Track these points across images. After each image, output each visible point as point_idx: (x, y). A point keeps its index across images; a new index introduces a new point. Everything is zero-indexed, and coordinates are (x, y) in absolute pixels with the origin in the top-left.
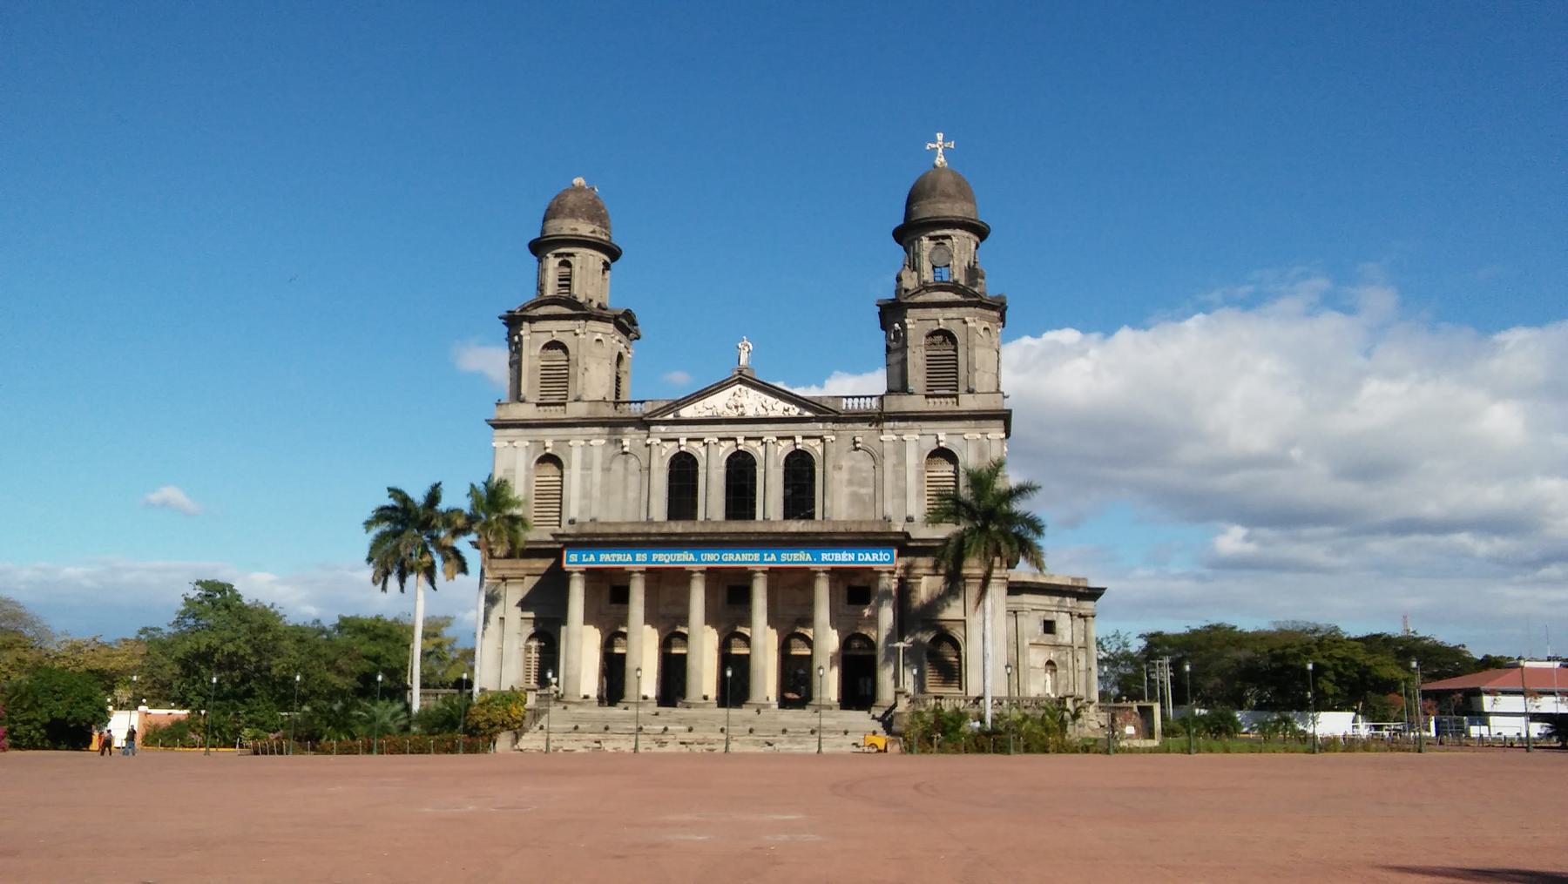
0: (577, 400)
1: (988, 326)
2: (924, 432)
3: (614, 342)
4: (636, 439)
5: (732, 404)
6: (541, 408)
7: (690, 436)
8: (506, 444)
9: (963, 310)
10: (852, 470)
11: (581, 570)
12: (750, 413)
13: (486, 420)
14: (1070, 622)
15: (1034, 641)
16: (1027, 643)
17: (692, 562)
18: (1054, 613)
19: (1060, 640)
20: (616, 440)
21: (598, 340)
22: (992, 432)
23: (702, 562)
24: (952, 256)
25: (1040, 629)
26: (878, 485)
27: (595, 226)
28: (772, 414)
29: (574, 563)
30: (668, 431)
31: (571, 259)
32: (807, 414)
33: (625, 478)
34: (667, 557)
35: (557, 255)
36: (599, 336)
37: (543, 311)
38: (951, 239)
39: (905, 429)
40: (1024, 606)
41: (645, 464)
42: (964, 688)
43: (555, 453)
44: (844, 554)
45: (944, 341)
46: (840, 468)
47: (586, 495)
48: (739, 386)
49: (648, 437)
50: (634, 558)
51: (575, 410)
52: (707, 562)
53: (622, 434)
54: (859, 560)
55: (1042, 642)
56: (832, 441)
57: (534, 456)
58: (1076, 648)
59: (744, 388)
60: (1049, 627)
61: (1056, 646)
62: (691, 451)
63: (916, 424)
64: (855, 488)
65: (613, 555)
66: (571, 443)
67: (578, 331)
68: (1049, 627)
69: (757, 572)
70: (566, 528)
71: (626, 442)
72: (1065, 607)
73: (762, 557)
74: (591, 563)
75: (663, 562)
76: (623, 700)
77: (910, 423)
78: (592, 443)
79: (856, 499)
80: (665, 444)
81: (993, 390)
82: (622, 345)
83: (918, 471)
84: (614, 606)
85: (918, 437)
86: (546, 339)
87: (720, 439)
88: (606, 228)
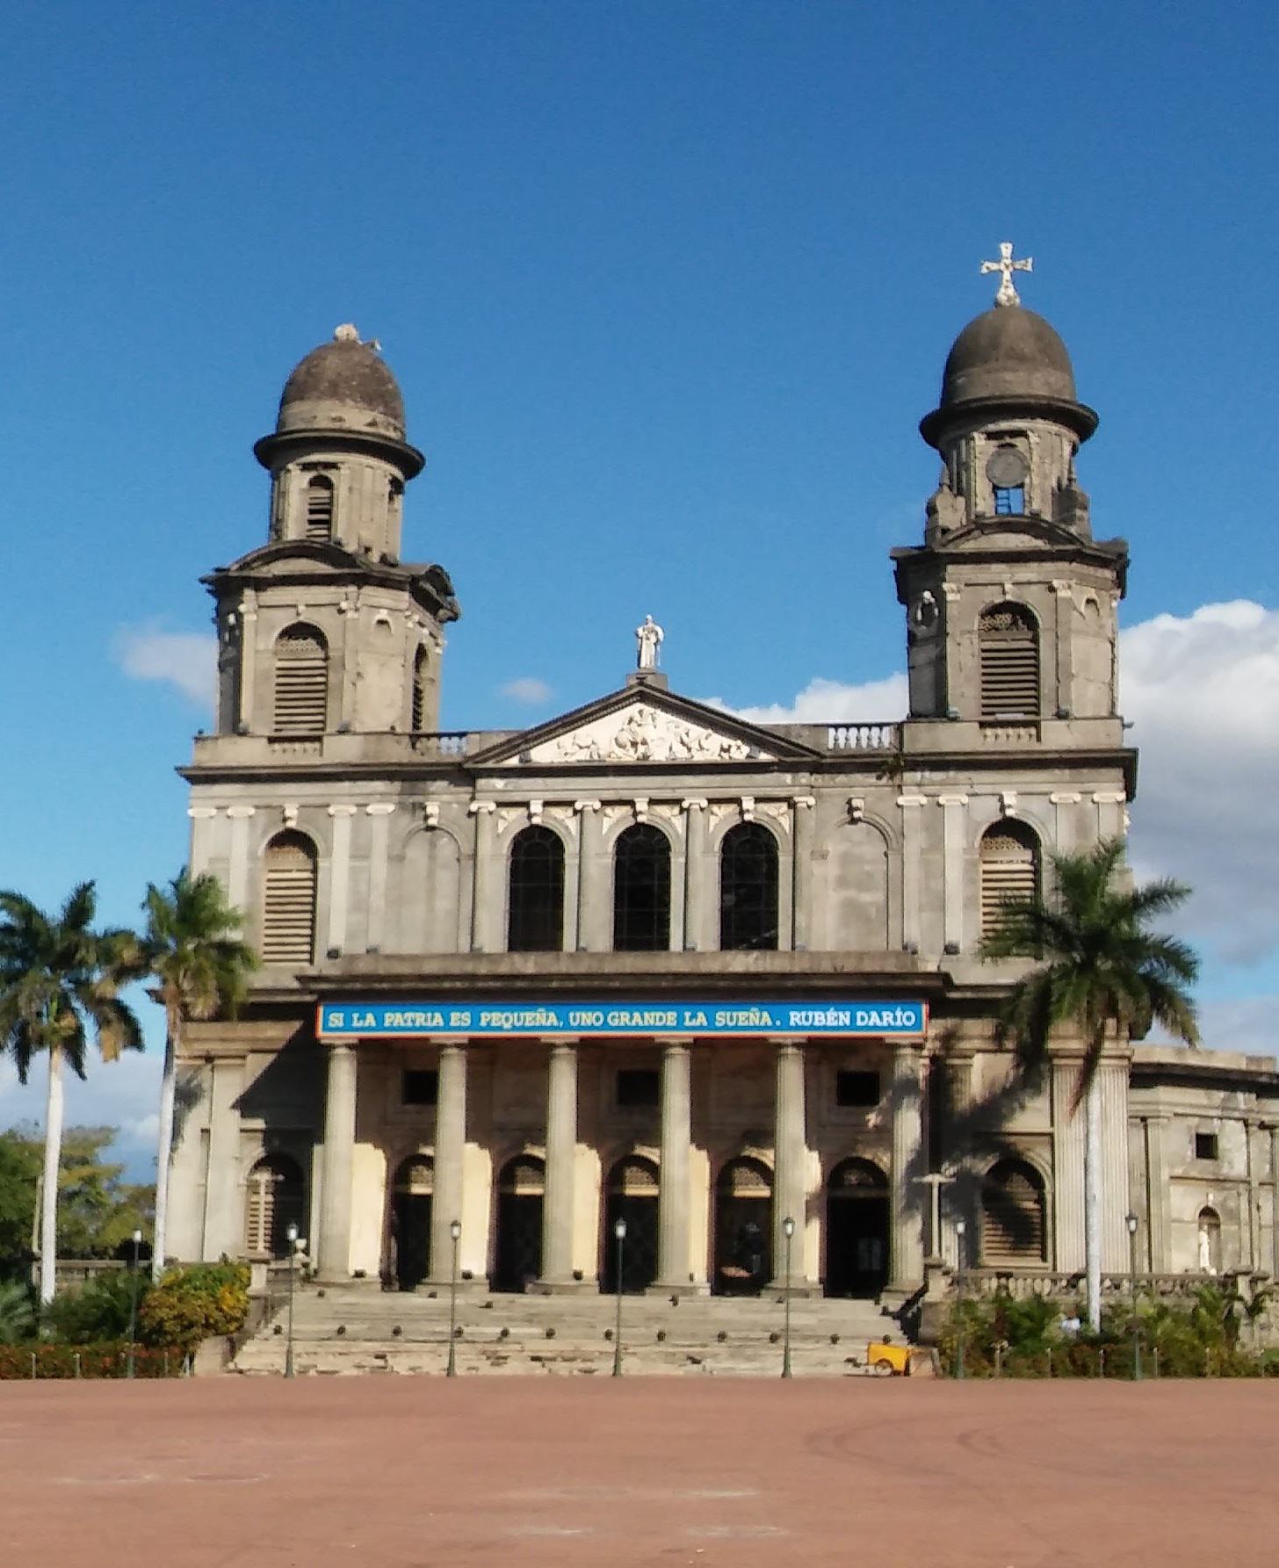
0: (343, 731)
1: (1094, 596)
2: (977, 789)
3: (410, 625)
4: (450, 803)
5: (626, 738)
6: (277, 746)
7: (550, 796)
8: (214, 812)
9: (1049, 566)
10: (846, 859)
11: (351, 1041)
12: (659, 756)
13: (177, 769)
15: (1179, 1171)
17: (552, 1028)
18: (1215, 1120)
19: (1225, 1171)
20: (414, 804)
21: (381, 622)
22: (1101, 790)
23: (572, 1029)
24: (1028, 468)
25: (1190, 1150)
26: (893, 887)
27: (375, 413)
28: (699, 757)
29: (337, 1029)
30: (510, 788)
31: (331, 474)
32: (764, 757)
33: (431, 874)
34: (507, 1019)
35: (306, 467)
37: (280, 568)
38: (1027, 436)
39: (942, 784)
40: (1161, 1108)
41: (467, 849)
42: (1050, 1257)
43: (303, 828)
44: (832, 1014)
45: (1014, 623)
46: (824, 856)
47: (359, 905)
48: (639, 706)
49: (473, 799)
50: (447, 1019)
51: (340, 751)
52: (580, 1028)
53: (425, 793)
54: (859, 1023)
55: (1193, 1174)
56: (809, 807)
57: (265, 832)
58: (1255, 1184)
59: (648, 709)
60: (1206, 1146)
61: (1219, 1182)
62: (551, 825)
63: (963, 776)
64: (851, 893)
65: (410, 1015)
66: (331, 810)
67: (344, 605)
68: (1206, 1146)
69: (671, 1046)
70: (323, 966)
71: (432, 808)
72: (1235, 1110)
73: (680, 1019)
74: (369, 1029)
75: (500, 1028)
76: (426, 1280)
77: (952, 774)
78: (369, 809)
79: (852, 912)
80: (504, 812)
81: (1104, 714)
82: (425, 631)
83: (967, 861)
84: (410, 1107)
85: (965, 800)
86: (286, 619)
87: (605, 803)
88: (396, 418)
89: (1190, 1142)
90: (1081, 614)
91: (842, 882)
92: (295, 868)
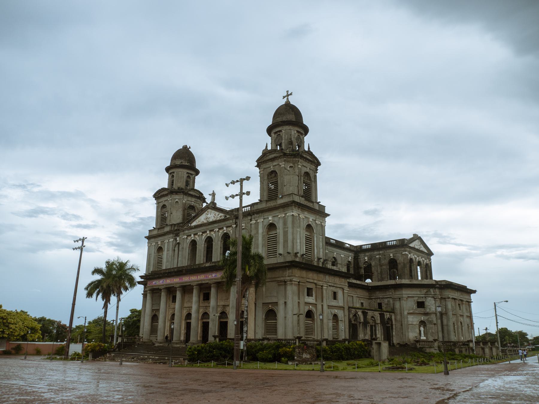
2: (265, 217)
12: (211, 220)
14: (434, 302)
15: (411, 311)
16: (406, 313)
19: (428, 311)
22: (289, 213)
25: (415, 306)
36: (177, 200)
40: (404, 295)
47: (167, 261)
60: (421, 305)
61: (426, 314)
68: (421, 305)
85: (262, 220)
89: (415, 304)
90: (288, 170)
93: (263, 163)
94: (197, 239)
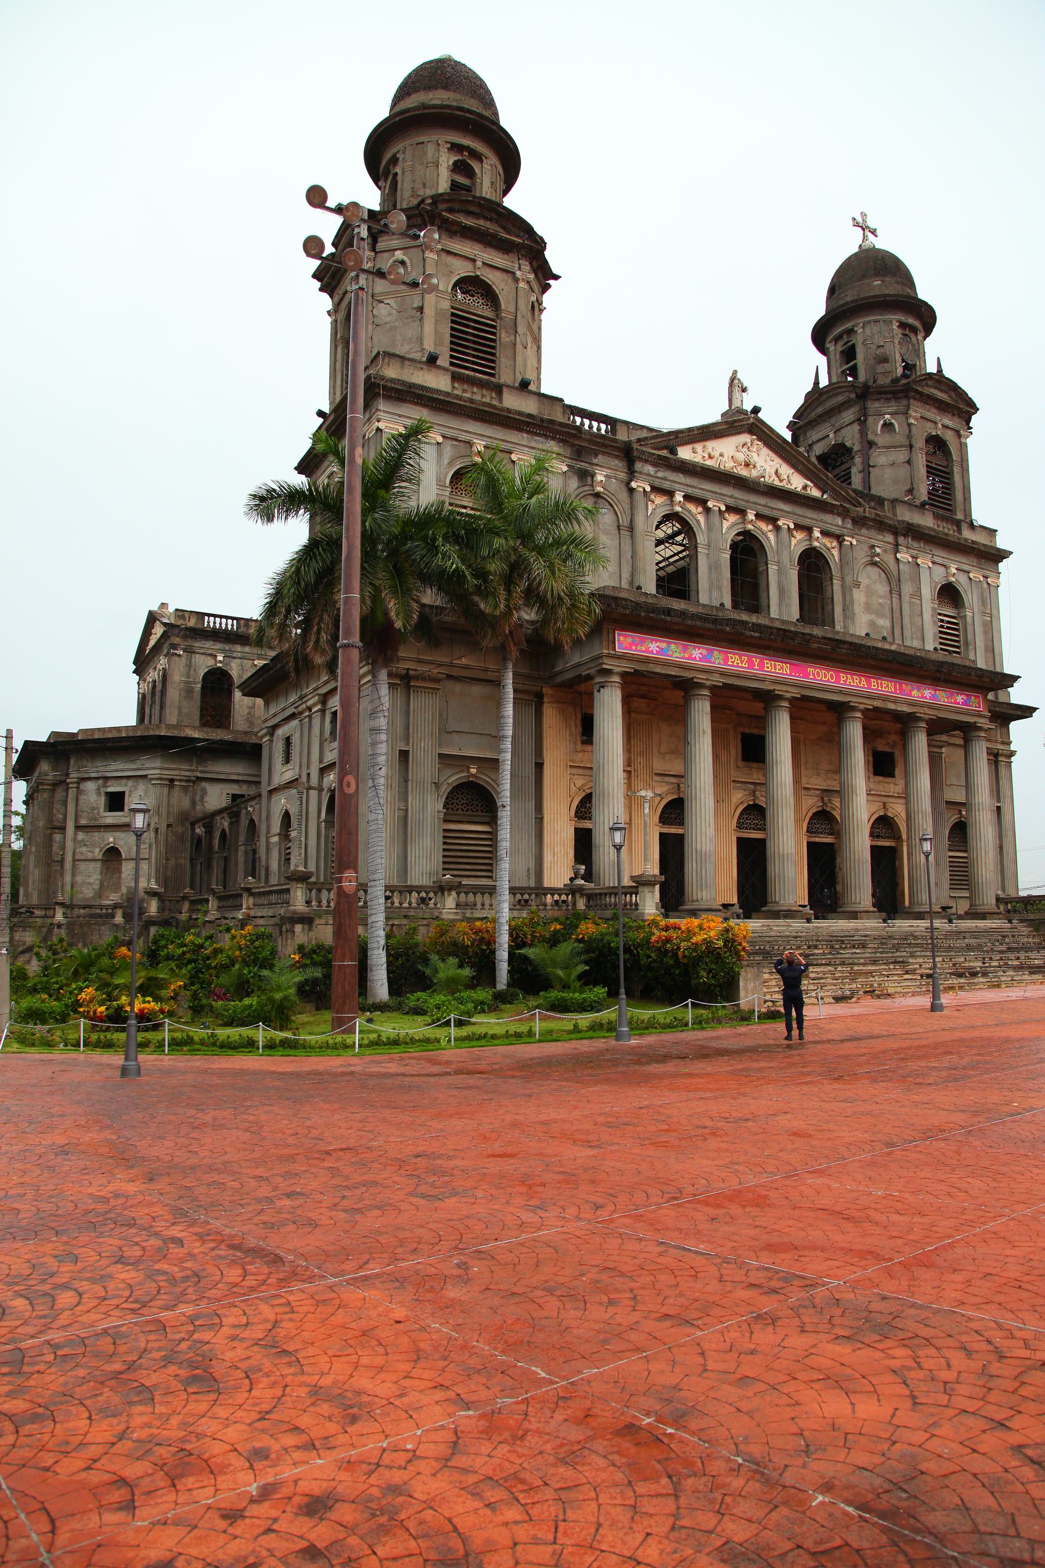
5: (741, 457)
31: (475, 166)
35: (455, 148)
48: (745, 438)
57: (451, 463)
64: (872, 617)
66: (514, 457)
85: (930, 565)
86: (463, 269)
91: (868, 608)
92: (471, 505)
93: (918, 396)
94: (698, 521)
